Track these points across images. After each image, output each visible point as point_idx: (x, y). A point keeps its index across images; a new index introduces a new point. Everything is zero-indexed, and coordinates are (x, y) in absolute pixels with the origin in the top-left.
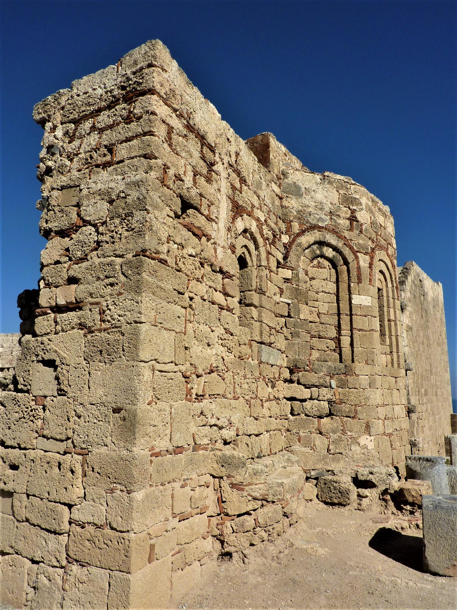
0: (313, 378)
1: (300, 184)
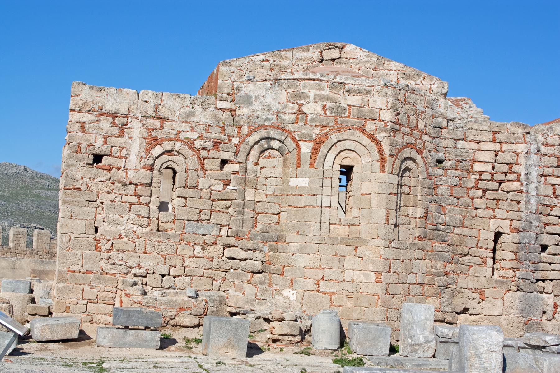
0: (249, 244)
1: (252, 94)
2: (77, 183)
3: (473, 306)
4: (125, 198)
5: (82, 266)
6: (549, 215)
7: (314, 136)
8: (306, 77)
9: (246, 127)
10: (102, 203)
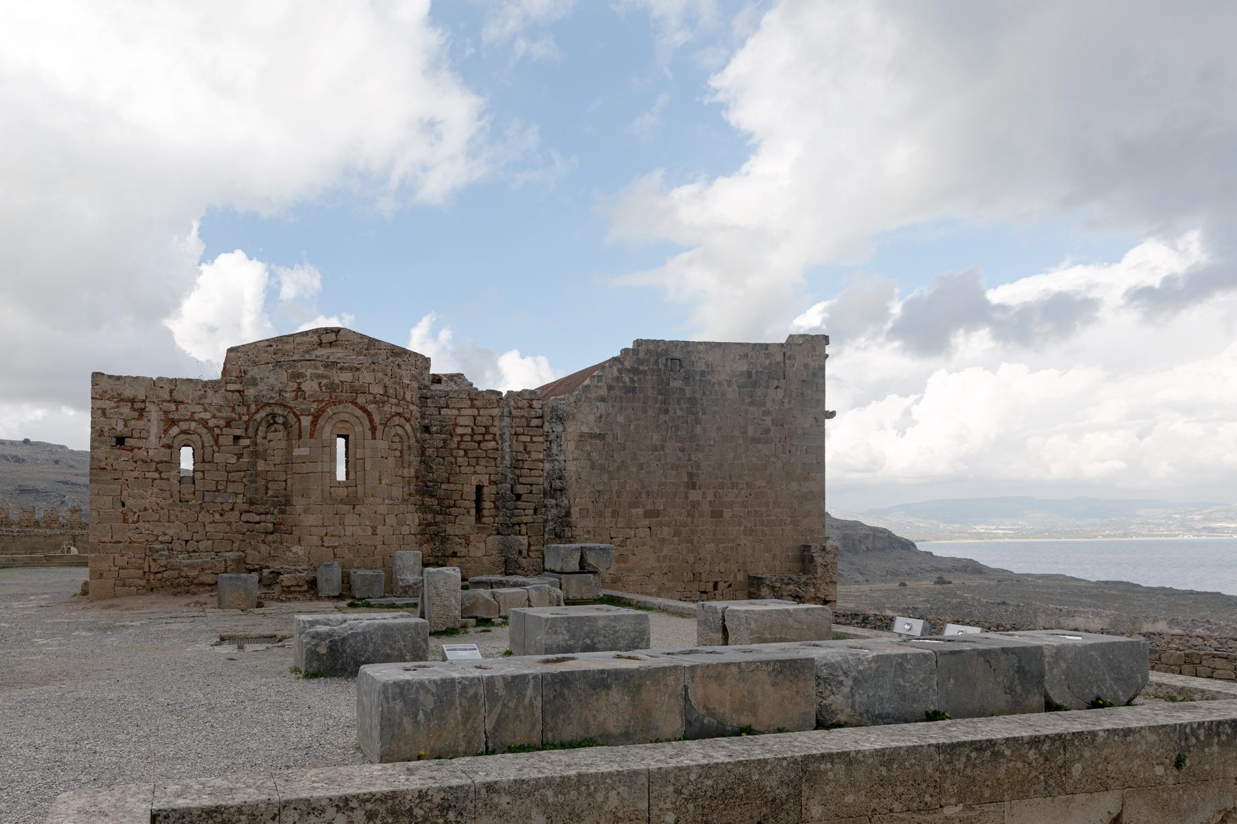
0: (261, 509)
1: (257, 376)
2: (102, 464)
3: (462, 551)
4: (148, 475)
5: (112, 537)
6: (522, 468)
7: (312, 410)
8: (303, 358)
9: (254, 406)
10: (127, 480)
